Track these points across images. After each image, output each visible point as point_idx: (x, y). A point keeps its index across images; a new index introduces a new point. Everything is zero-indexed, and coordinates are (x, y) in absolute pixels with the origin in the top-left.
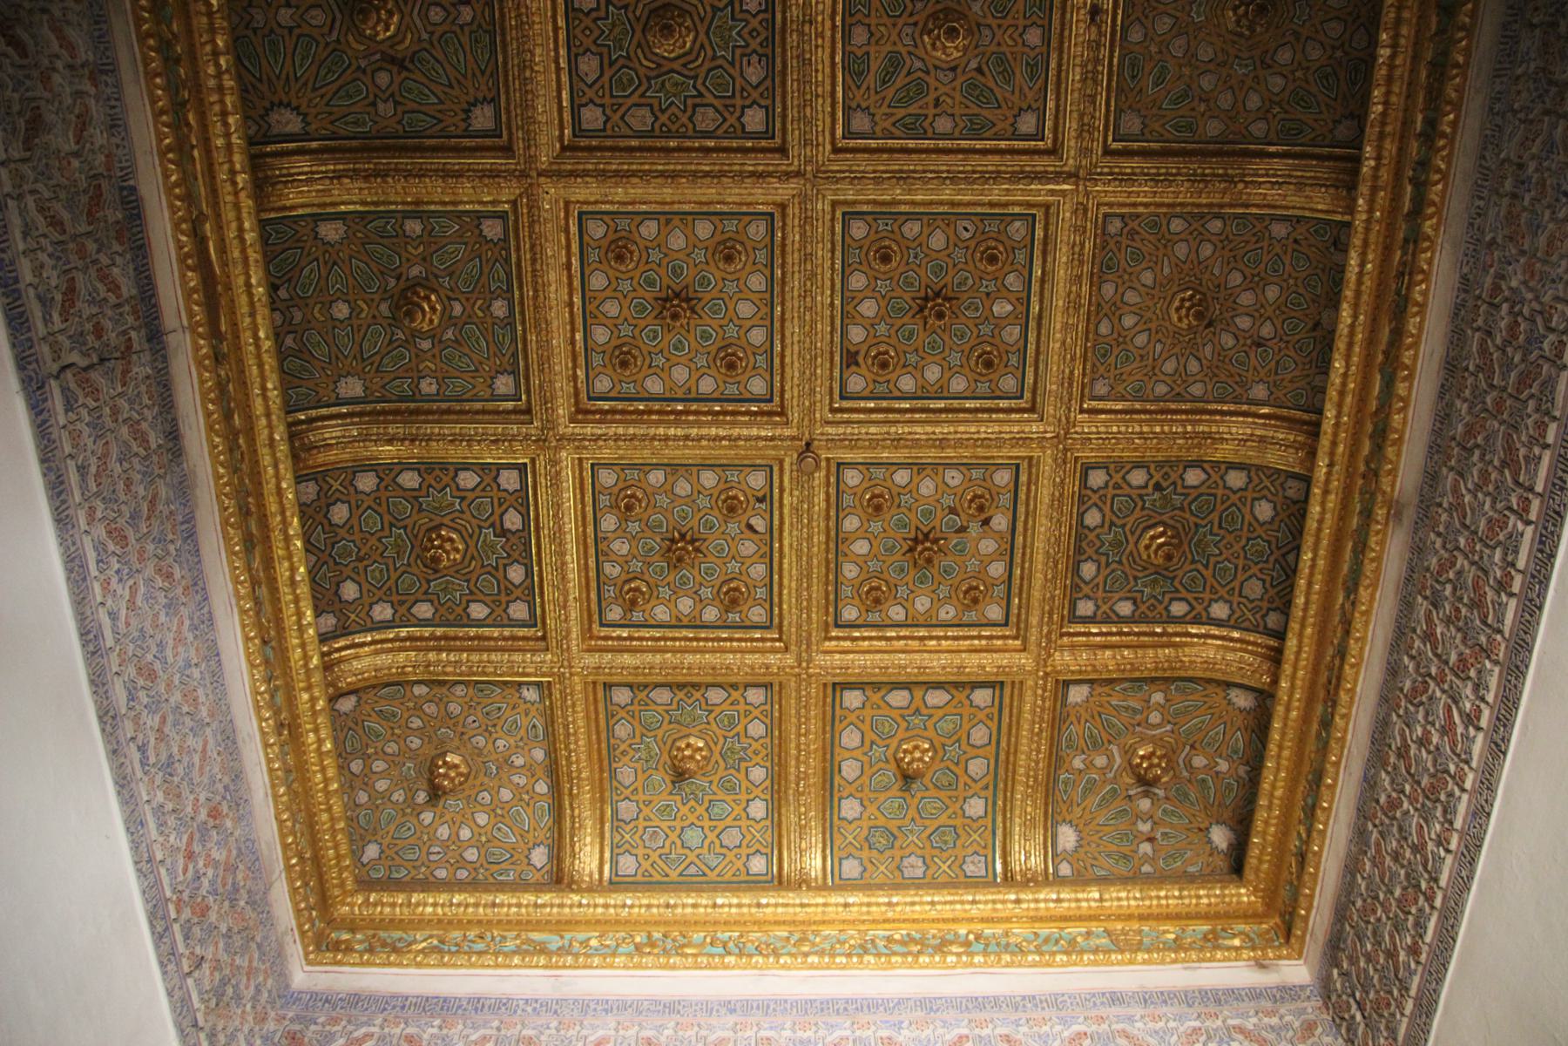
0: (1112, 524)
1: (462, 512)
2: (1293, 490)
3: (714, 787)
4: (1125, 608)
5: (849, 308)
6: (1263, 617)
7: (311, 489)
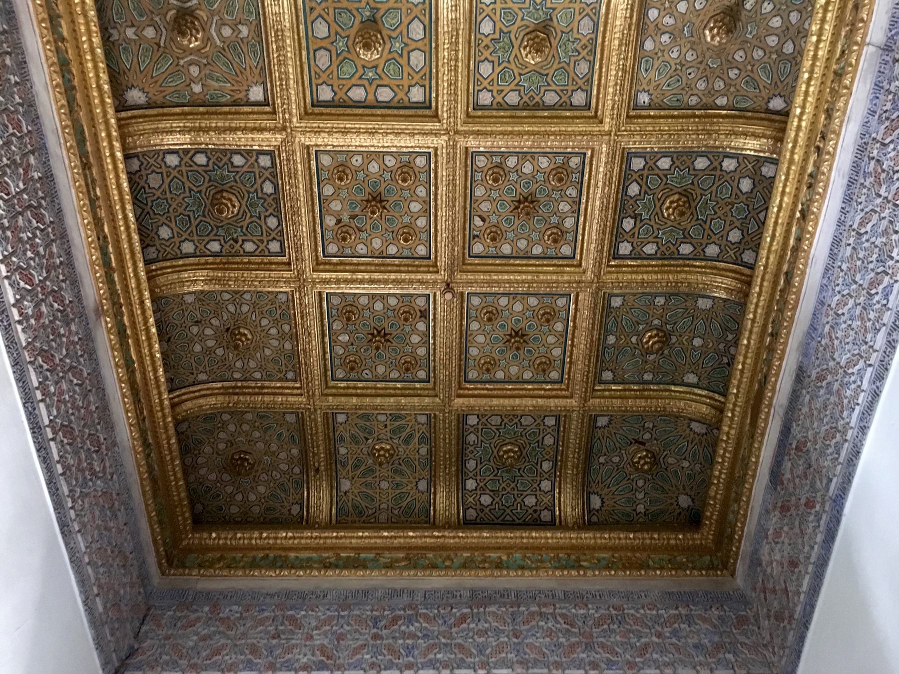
0: (259, 218)
1: (658, 229)
2: (152, 253)
3: (520, 15)
4: (238, 160)
5: (425, 339)
6: (142, 164)
7: (748, 257)
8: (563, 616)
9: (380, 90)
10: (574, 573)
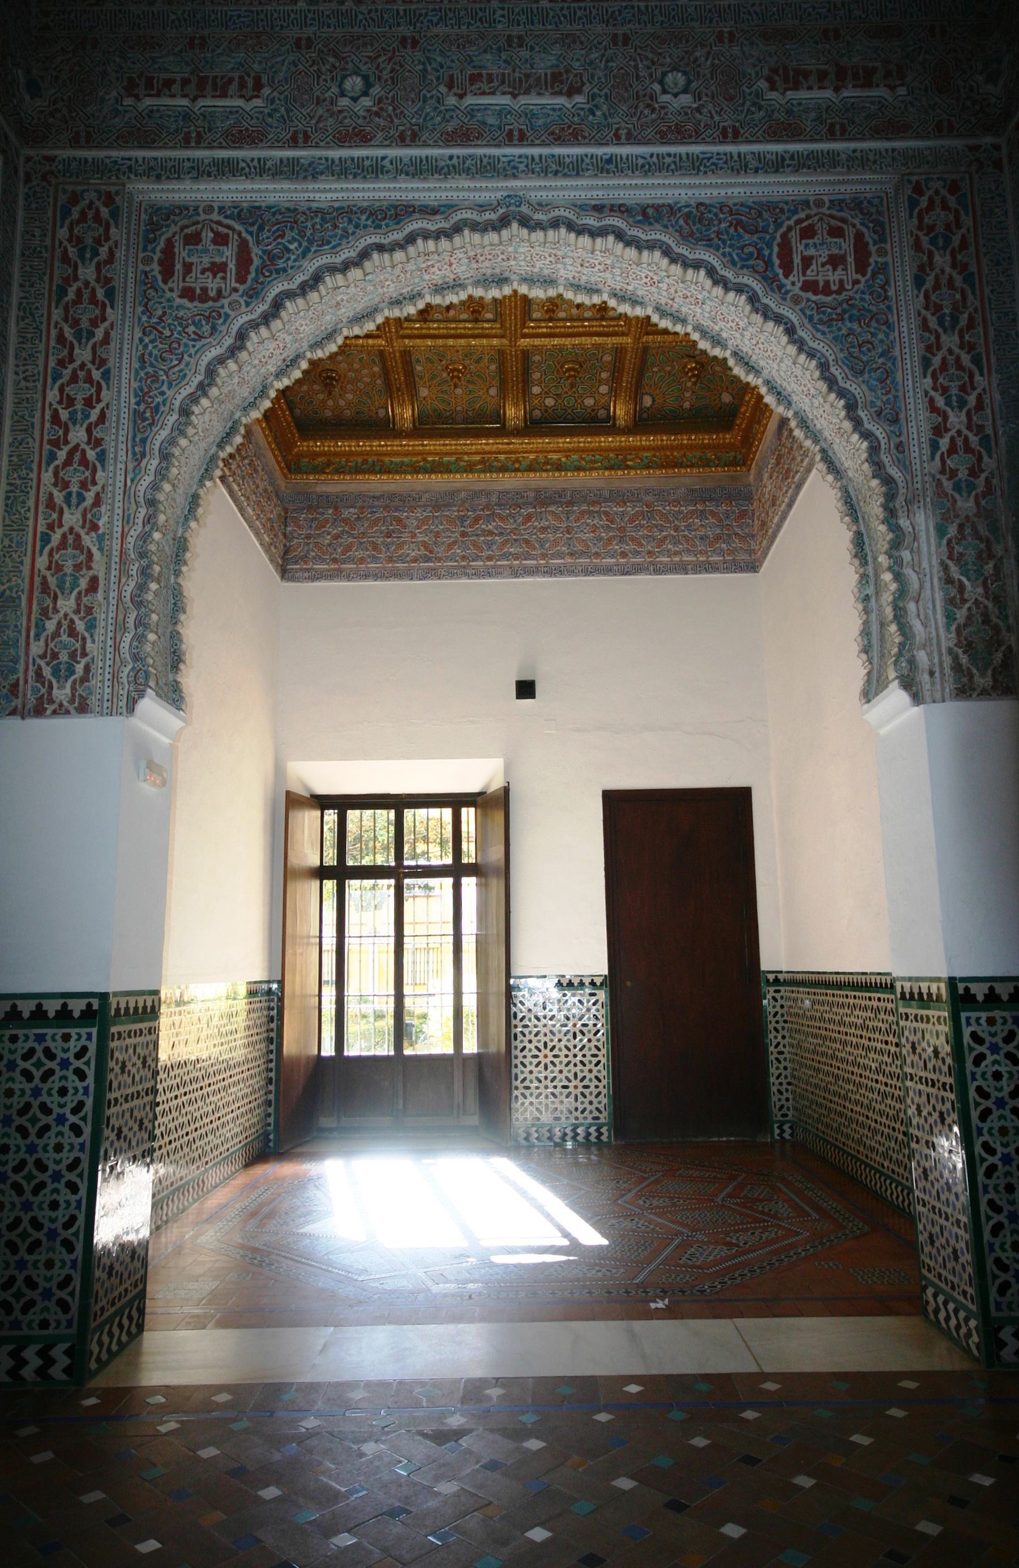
8: (606, 513)
10: (620, 473)
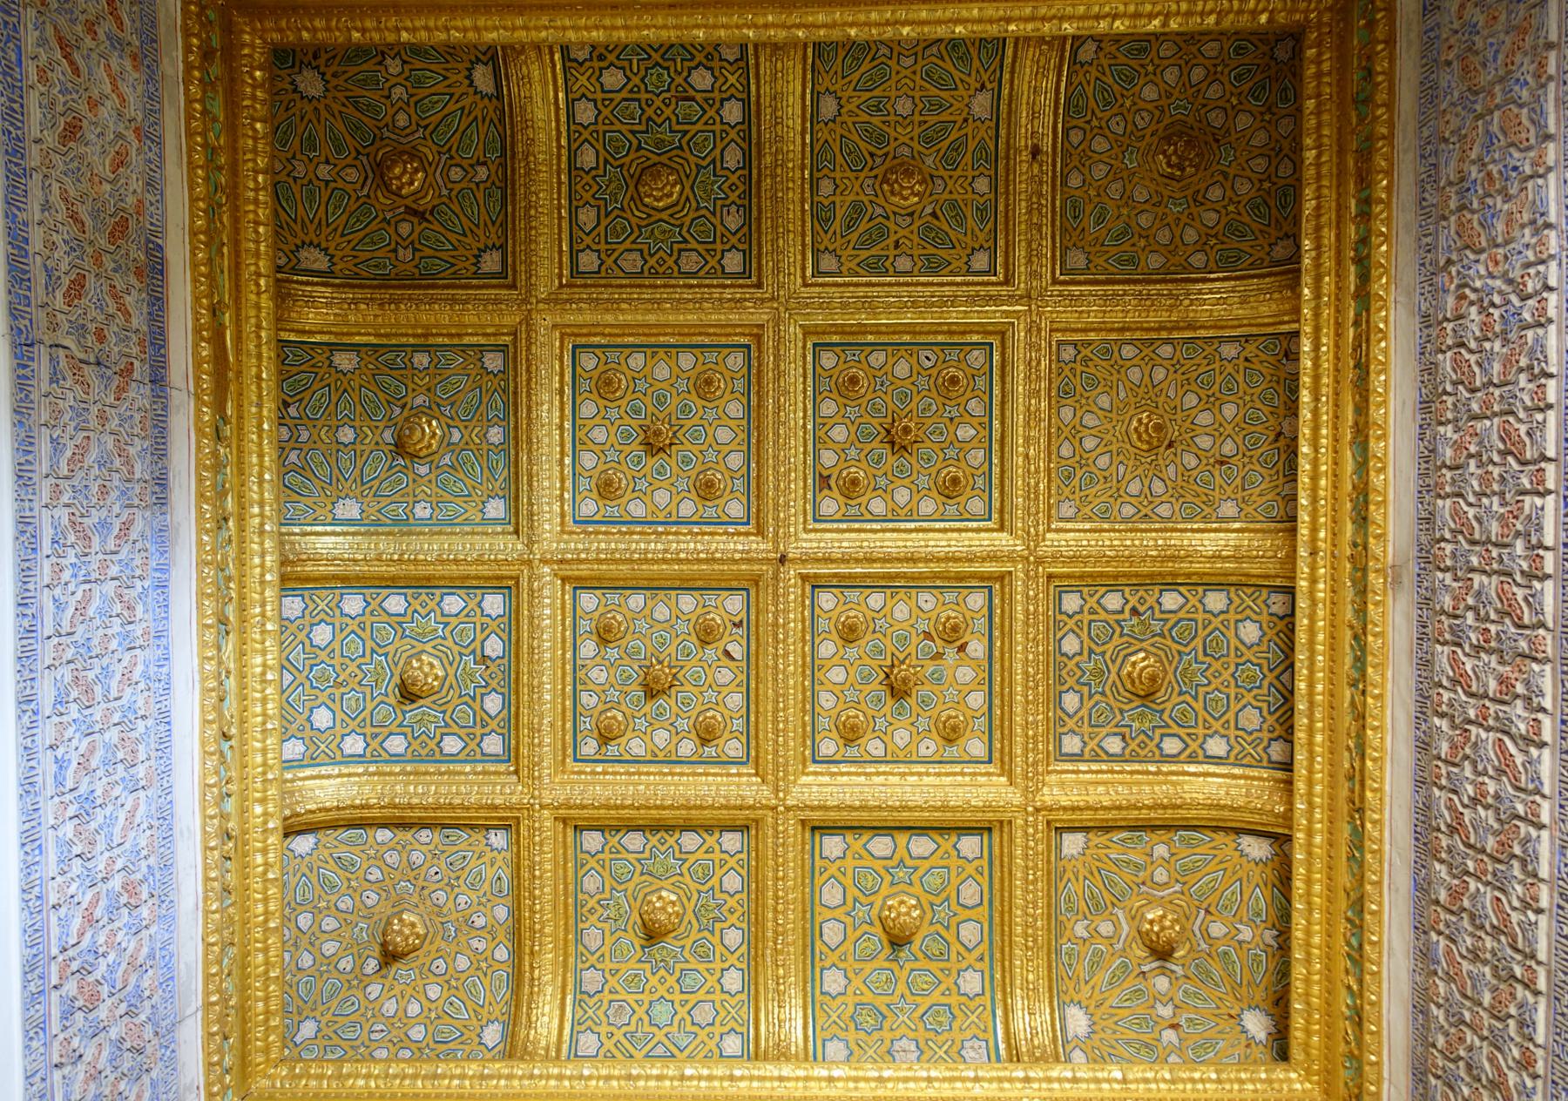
3: (686, 954)
4: (1114, 745)
9: (888, 853)
